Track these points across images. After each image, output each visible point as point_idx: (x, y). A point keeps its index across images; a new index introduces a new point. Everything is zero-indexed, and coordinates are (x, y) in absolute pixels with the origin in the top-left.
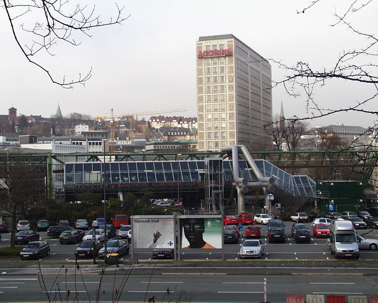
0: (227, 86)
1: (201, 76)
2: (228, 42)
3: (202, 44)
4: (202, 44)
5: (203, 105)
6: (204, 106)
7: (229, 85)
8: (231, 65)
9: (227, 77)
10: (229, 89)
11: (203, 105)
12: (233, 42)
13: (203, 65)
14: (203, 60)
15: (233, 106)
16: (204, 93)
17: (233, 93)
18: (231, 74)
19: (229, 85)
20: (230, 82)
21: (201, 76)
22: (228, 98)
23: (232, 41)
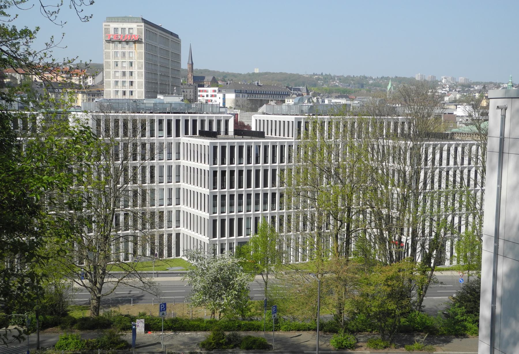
0: (136, 73)
1: (109, 60)
2: (138, 26)
3: (109, 25)
4: (109, 25)
5: (110, 91)
6: (112, 92)
7: (138, 72)
8: (140, 51)
9: (136, 63)
10: (138, 75)
11: (110, 91)
12: (143, 27)
13: (111, 48)
14: (111, 44)
15: (142, 94)
16: (111, 78)
17: (142, 80)
18: (140, 61)
19: (138, 72)
20: (139, 68)
21: (109, 60)
22: (136, 85)
23: (141, 26)
